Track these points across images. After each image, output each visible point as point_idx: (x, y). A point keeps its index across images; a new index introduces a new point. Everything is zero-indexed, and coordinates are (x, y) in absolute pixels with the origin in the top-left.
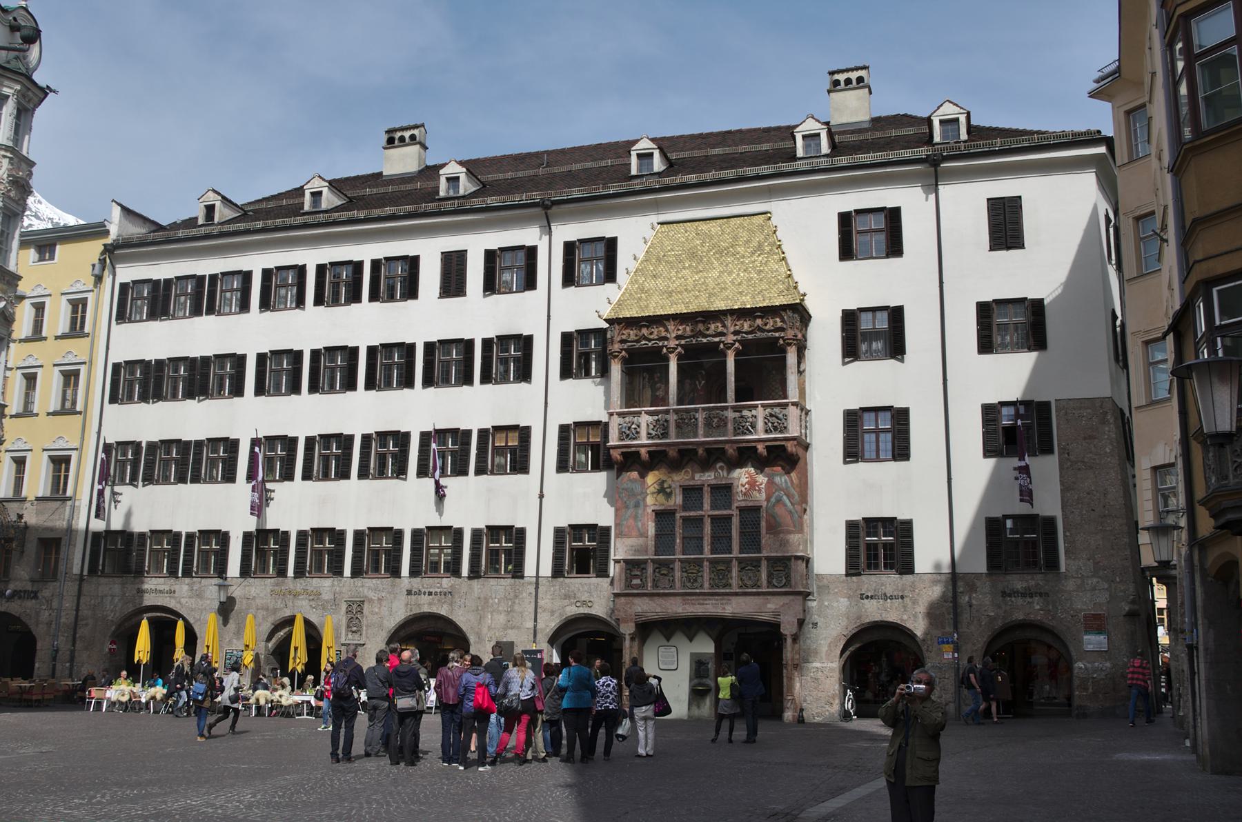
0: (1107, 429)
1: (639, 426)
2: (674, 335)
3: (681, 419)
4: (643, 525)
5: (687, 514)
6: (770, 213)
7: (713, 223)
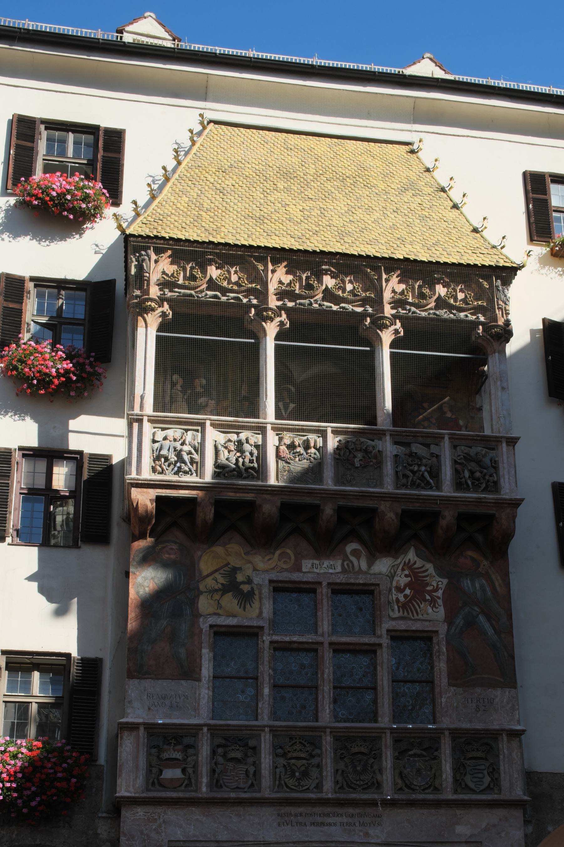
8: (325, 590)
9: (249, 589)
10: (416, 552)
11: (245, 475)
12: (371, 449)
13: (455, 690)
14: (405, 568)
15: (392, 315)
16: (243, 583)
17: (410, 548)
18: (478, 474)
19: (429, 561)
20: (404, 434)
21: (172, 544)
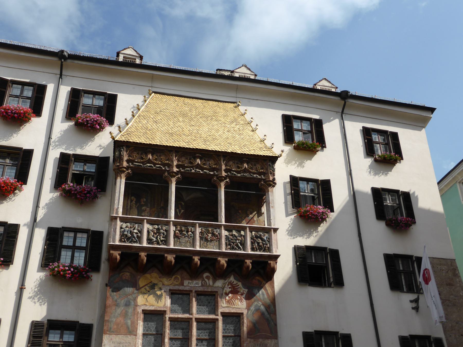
0: (458, 280)
1: (141, 232)
4: (133, 323)
5: (176, 316)
8: (194, 294)
9: (160, 294)
13: (250, 340)
14: (229, 284)
15: (225, 175)
17: (231, 275)
19: (240, 281)
21: (128, 273)
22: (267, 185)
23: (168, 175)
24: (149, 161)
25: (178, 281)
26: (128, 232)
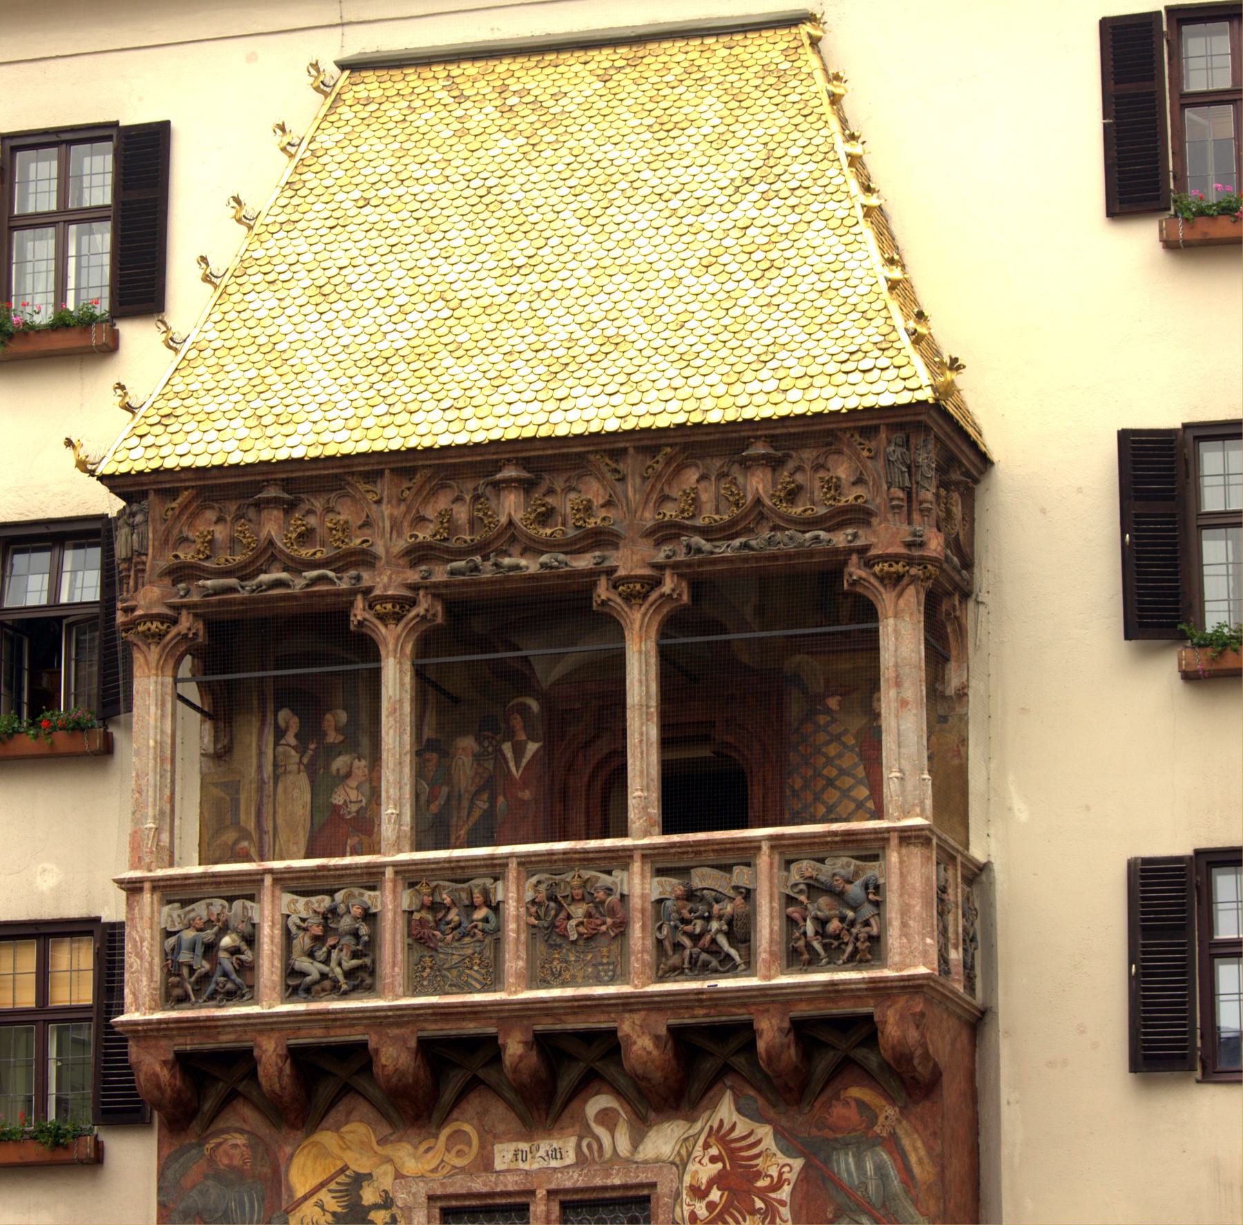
1: (251, 939)
2: (401, 544)
3: (434, 907)
6: (810, 18)
7: (572, 62)
9: (388, 1220)
10: (736, 1103)
11: (344, 987)
12: (601, 895)
14: (712, 1141)
16: (376, 1207)
18: (834, 925)
19: (761, 1119)
20: (673, 850)
22: (881, 579)
23: (368, 615)
24: (268, 555)
25: (466, 1149)
26: (193, 950)
